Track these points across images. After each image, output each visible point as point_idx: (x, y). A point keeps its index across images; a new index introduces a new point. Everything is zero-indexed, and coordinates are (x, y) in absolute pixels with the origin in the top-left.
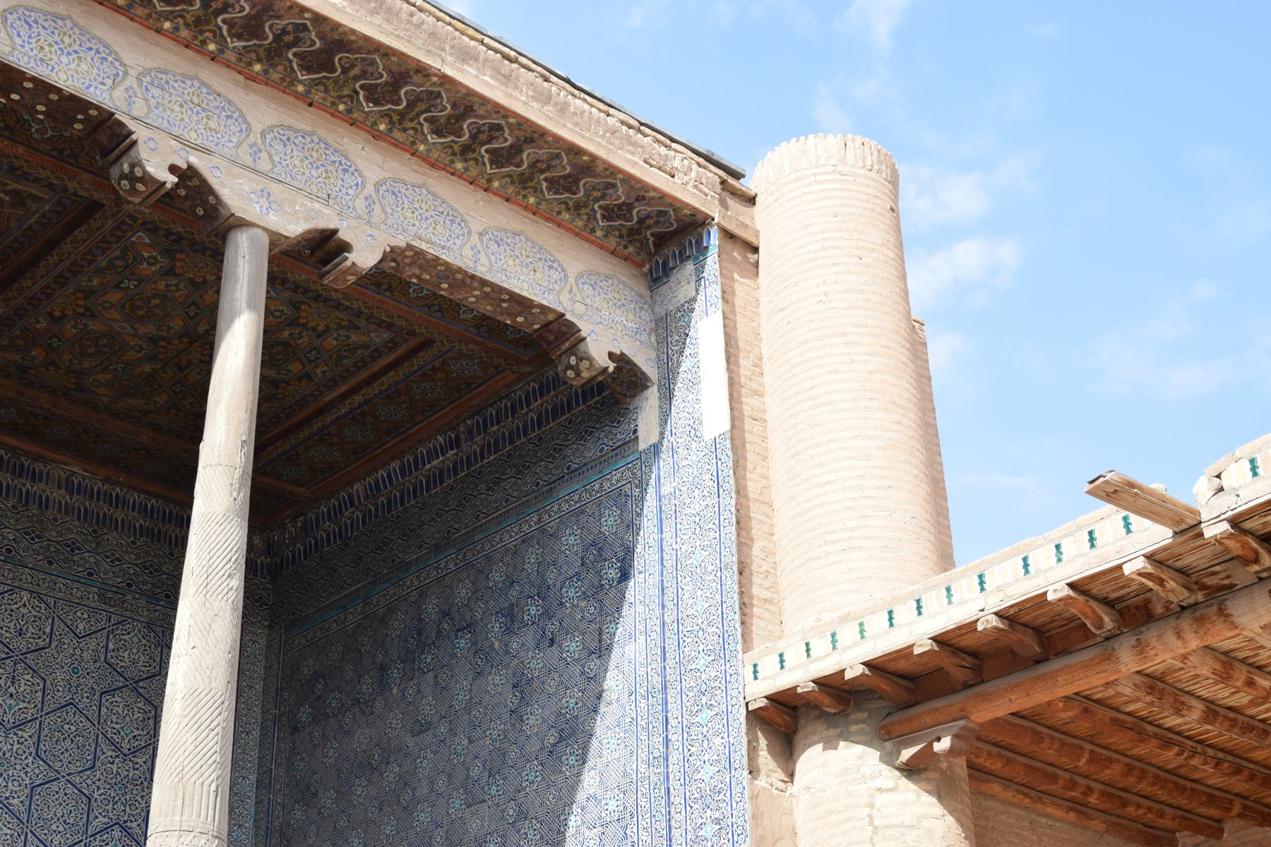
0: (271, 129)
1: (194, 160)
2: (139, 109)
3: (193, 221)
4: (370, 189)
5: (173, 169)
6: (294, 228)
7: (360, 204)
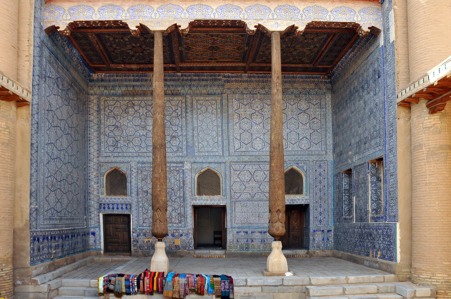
0: (276, 8)
1: (260, 23)
2: (246, 17)
3: (262, 34)
4: (301, 12)
5: (255, 27)
6: (283, 28)
7: (299, 17)
